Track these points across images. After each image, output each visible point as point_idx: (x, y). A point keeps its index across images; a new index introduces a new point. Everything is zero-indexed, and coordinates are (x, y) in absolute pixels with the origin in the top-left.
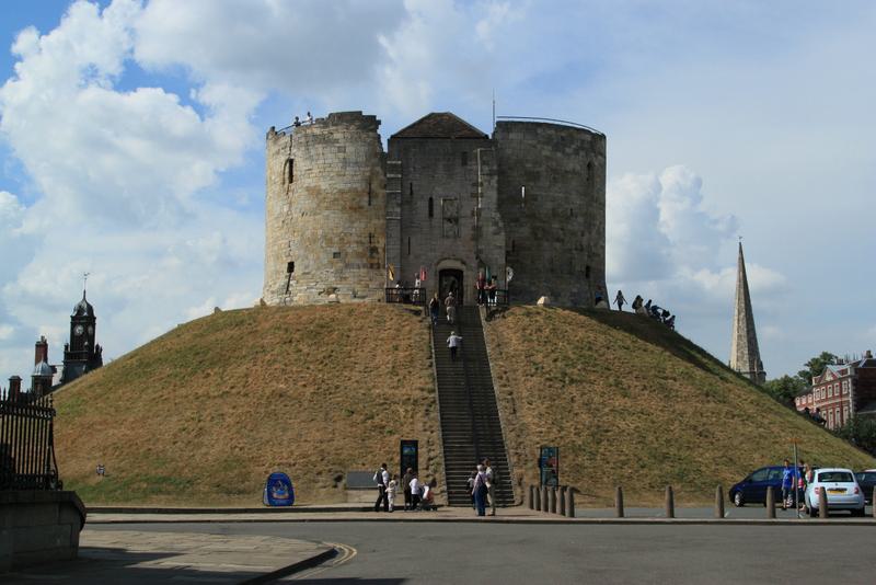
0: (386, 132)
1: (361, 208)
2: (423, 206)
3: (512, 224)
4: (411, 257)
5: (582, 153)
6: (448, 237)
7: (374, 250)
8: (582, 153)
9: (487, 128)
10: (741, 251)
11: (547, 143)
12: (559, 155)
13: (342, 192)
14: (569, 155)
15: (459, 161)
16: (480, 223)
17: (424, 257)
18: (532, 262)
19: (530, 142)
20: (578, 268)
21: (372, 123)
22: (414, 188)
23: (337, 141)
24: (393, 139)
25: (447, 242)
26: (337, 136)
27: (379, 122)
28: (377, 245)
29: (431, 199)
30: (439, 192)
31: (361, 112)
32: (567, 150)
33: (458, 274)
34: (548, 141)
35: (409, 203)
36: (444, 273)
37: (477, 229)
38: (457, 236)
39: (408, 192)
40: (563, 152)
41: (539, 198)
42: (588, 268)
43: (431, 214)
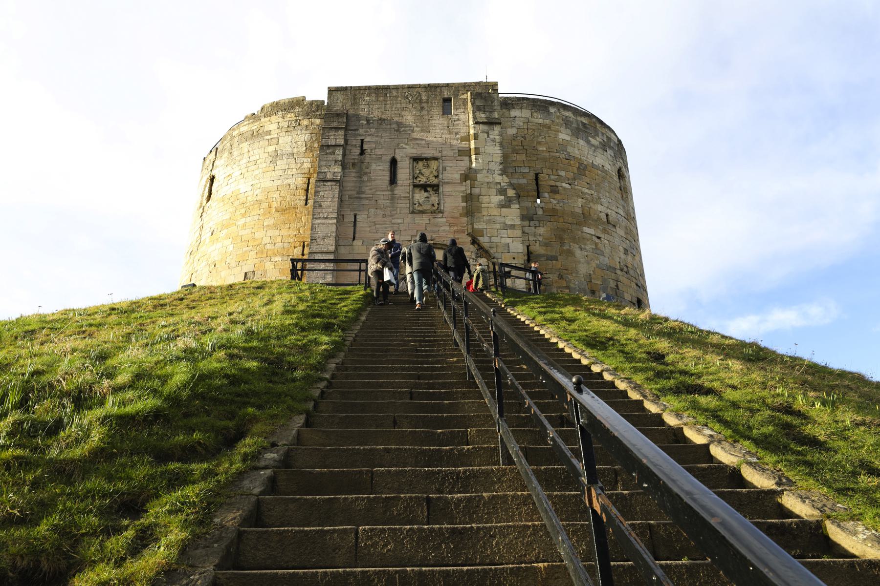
2: (379, 171)
3: (526, 223)
5: (610, 152)
6: (422, 212)
8: (610, 152)
12: (582, 142)
14: (596, 147)
15: (437, 111)
16: (476, 191)
18: (561, 277)
19: (541, 121)
22: (365, 147)
29: (394, 162)
32: (593, 141)
34: (567, 123)
37: (469, 198)
38: (437, 211)
39: (357, 151)
40: (588, 142)
43: (393, 180)
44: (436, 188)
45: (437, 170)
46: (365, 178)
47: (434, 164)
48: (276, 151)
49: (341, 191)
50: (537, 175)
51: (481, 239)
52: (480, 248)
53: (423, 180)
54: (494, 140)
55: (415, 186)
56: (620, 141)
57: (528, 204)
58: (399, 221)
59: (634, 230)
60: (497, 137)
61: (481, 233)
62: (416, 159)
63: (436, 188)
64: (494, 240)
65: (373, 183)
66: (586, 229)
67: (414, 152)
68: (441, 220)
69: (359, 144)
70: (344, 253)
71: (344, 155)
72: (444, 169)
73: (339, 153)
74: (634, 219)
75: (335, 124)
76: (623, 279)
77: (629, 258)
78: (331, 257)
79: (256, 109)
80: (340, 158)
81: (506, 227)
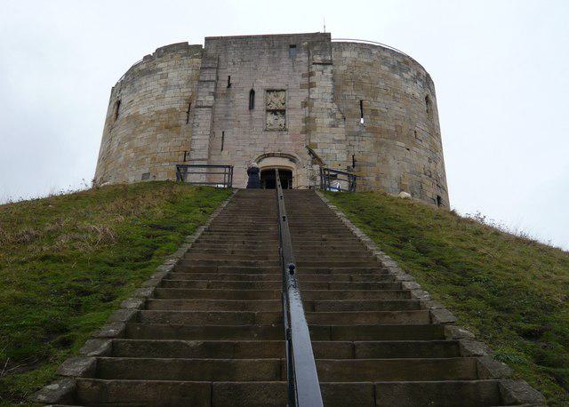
1: (177, 126)
3: (352, 138)
4: (225, 152)
6: (272, 130)
8: (419, 83)
11: (384, 64)
12: (397, 77)
13: (159, 113)
15: (285, 54)
16: (313, 115)
18: (378, 179)
19: (366, 60)
20: (430, 195)
22: (232, 81)
26: (160, 65)
29: (252, 93)
30: (261, 84)
31: (187, 43)
32: (405, 75)
33: (286, 175)
34: (385, 61)
35: (226, 95)
37: (307, 120)
38: (283, 129)
40: (401, 76)
41: (379, 113)
43: (252, 106)
44: (283, 112)
45: (284, 99)
46: (231, 105)
47: (282, 95)
48: (166, 83)
49: (213, 114)
50: (361, 101)
52: (315, 157)
53: (273, 107)
54: (327, 77)
55: (268, 111)
56: (428, 75)
57: (352, 122)
58: (255, 137)
59: (438, 144)
61: (316, 146)
62: (269, 91)
63: (283, 112)
64: (326, 151)
65: (237, 109)
66: (398, 143)
67: (268, 86)
68: (286, 136)
69: (227, 79)
70: (215, 160)
71: (216, 88)
72: (290, 98)
73: (212, 86)
74: (438, 135)
75: (210, 65)
76: (428, 182)
77: (432, 165)
78: (205, 163)
79: (151, 51)
80: (213, 90)
81: (335, 141)
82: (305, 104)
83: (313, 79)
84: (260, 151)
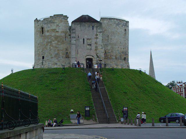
0: (70, 21)
2: (82, 40)
4: (78, 55)
7: (67, 53)
8: (124, 26)
9: (99, 20)
10: (151, 55)
12: (118, 27)
17: (82, 55)
20: (122, 58)
21: (66, 17)
23: (56, 23)
24: (73, 22)
25: (89, 51)
26: (56, 21)
27: (68, 17)
28: (68, 52)
30: (86, 37)
36: (87, 59)
37: (96, 47)
38: (91, 49)
40: (119, 26)
42: (125, 58)
43: (84, 43)
44: (91, 45)
47: (90, 40)
51: (97, 54)
52: (98, 56)
60: (101, 35)
79: (52, 15)
82: (96, 43)
83: (97, 36)
84: (86, 54)
